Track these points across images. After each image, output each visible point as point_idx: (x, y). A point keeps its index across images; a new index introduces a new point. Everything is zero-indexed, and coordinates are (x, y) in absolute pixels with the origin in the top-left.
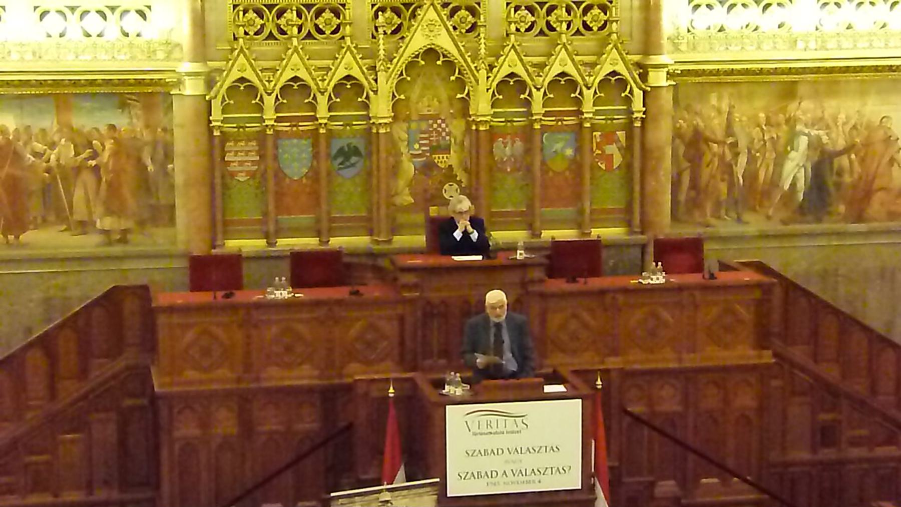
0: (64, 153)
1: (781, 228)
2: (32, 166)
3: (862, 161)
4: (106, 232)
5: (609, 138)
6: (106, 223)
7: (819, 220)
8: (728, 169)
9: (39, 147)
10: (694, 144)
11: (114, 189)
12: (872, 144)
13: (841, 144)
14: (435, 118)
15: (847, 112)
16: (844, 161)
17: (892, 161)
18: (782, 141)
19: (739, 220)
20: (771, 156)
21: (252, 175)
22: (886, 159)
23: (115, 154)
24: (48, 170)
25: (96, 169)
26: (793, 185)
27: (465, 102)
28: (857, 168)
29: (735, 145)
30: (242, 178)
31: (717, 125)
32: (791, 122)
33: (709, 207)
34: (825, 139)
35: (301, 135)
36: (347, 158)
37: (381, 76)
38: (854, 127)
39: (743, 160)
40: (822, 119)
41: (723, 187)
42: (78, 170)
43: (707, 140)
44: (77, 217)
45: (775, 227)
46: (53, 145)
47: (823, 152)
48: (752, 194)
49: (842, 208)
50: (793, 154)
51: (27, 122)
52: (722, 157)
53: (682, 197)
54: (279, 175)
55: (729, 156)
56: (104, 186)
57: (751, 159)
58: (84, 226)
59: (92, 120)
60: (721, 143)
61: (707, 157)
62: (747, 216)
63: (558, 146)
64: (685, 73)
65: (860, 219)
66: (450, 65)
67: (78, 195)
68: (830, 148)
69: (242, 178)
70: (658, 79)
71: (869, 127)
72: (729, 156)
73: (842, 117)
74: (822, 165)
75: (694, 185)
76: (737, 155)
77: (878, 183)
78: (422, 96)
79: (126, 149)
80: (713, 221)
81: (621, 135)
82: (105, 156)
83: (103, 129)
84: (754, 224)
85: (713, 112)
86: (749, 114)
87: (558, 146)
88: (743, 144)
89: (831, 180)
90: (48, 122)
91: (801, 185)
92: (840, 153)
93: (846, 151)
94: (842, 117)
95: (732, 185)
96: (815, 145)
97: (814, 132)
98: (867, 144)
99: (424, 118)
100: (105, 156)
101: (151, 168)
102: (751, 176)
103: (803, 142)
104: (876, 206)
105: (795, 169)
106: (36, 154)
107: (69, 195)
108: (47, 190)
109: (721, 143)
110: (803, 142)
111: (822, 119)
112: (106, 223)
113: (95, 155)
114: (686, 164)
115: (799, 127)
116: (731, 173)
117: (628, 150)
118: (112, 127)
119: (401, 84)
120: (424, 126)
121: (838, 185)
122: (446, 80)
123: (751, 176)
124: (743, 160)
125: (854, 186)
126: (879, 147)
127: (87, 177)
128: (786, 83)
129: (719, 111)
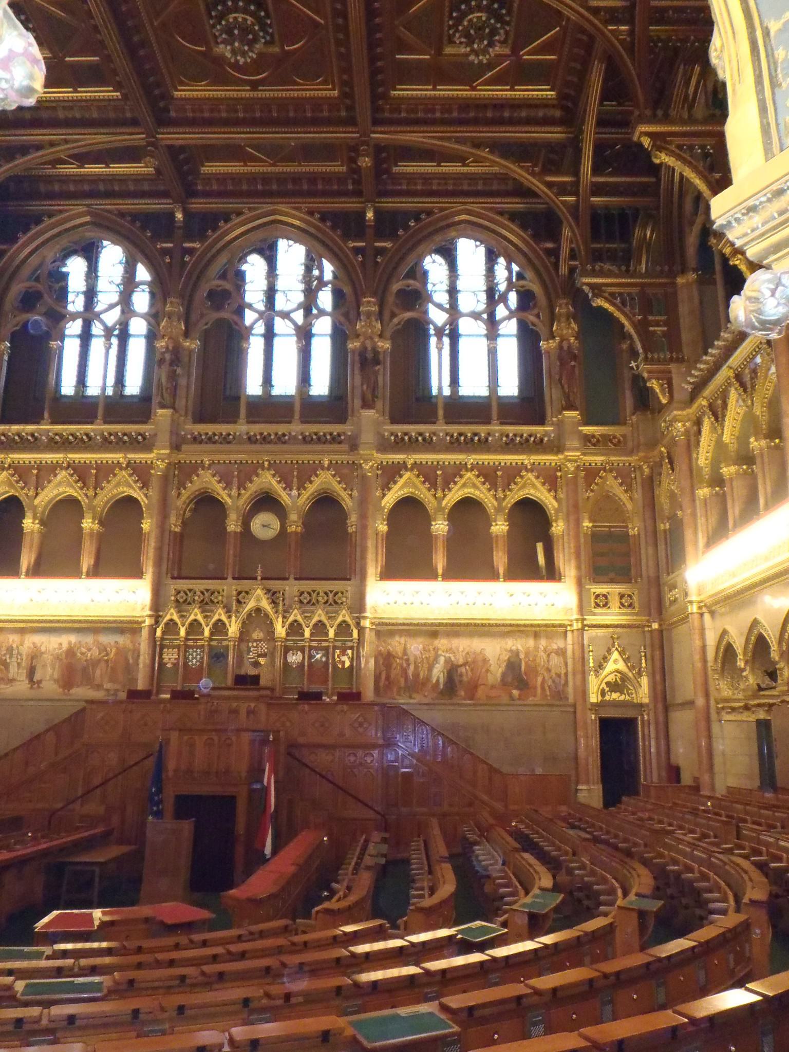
0: (95, 653)
1: (432, 702)
2: (80, 659)
3: (472, 670)
4: (108, 690)
5: (344, 653)
6: (108, 685)
7: (451, 699)
8: (405, 671)
9: (84, 650)
10: (386, 660)
11: (113, 669)
12: (477, 662)
13: (461, 661)
14: (260, 641)
15: (464, 646)
16: (463, 670)
17: (488, 671)
18: (431, 659)
19: (411, 697)
20: (426, 665)
21: (174, 664)
22: (483, 670)
23: (116, 654)
24: (86, 661)
25: (107, 661)
26: (438, 681)
27: (273, 633)
28: (470, 673)
29: (407, 660)
30: (169, 666)
31: (399, 650)
32: (436, 650)
33: (395, 690)
34: (453, 659)
35: (198, 647)
36: (218, 658)
37: (233, 618)
38: (468, 653)
39: (412, 667)
40: (451, 649)
41: (402, 681)
42: (99, 661)
43: (394, 657)
44: (96, 683)
45: (426, 701)
46: (89, 650)
47: (452, 665)
48: (416, 685)
49: (463, 693)
50: (437, 665)
51: (80, 639)
52: (401, 666)
53: (381, 684)
54: (186, 665)
55: (405, 665)
56: (109, 669)
57: (416, 668)
58: (99, 687)
59: (107, 639)
60: (401, 659)
61: (394, 665)
62: (414, 695)
63: (318, 656)
64: (379, 624)
65: (472, 698)
66: (267, 615)
67: (98, 672)
68: (455, 663)
69: (169, 666)
70: (366, 623)
71: (474, 653)
72: (405, 665)
73: (461, 649)
74: (452, 671)
75: (388, 678)
76: (409, 665)
77: (479, 682)
78: (254, 630)
79: (121, 652)
80: (397, 697)
81: (349, 652)
82: (112, 656)
83: (112, 643)
84: (417, 698)
85: (396, 644)
86: (415, 647)
87: (318, 656)
88: (412, 659)
89: (456, 679)
90: (89, 639)
91: (442, 681)
92: (461, 666)
93: (465, 664)
94: (461, 649)
95: (406, 679)
96: (448, 661)
97: (447, 655)
98: (474, 662)
99: (256, 641)
100: (112, 656)
101: (131, 661)
102: (416, 675)
103: (442, 660)
104: (480, 693)
105: (438, 673)
106: (82, 654)
107: (94, 673)
108: (85, 669)
109: (401, 659)
110: (442, 660)
111: (451, 649)
112: (108, 685)
113: (107, 655)
114: (383, 668)
115: (440, 652)
116: (406, 673)
117: (352, 661)
118: (116, 642)
119: (244, 623)
120: (255, 644)
121: (461, 682)
122: (265, 623)
123: (416, 675)
124: (412, 667)
125: (469, 682)
126: (480, 664)
127: (103, 664)
128: (433, 631)
129: (400, 643)
